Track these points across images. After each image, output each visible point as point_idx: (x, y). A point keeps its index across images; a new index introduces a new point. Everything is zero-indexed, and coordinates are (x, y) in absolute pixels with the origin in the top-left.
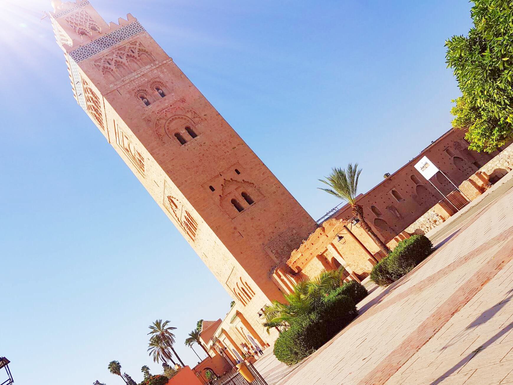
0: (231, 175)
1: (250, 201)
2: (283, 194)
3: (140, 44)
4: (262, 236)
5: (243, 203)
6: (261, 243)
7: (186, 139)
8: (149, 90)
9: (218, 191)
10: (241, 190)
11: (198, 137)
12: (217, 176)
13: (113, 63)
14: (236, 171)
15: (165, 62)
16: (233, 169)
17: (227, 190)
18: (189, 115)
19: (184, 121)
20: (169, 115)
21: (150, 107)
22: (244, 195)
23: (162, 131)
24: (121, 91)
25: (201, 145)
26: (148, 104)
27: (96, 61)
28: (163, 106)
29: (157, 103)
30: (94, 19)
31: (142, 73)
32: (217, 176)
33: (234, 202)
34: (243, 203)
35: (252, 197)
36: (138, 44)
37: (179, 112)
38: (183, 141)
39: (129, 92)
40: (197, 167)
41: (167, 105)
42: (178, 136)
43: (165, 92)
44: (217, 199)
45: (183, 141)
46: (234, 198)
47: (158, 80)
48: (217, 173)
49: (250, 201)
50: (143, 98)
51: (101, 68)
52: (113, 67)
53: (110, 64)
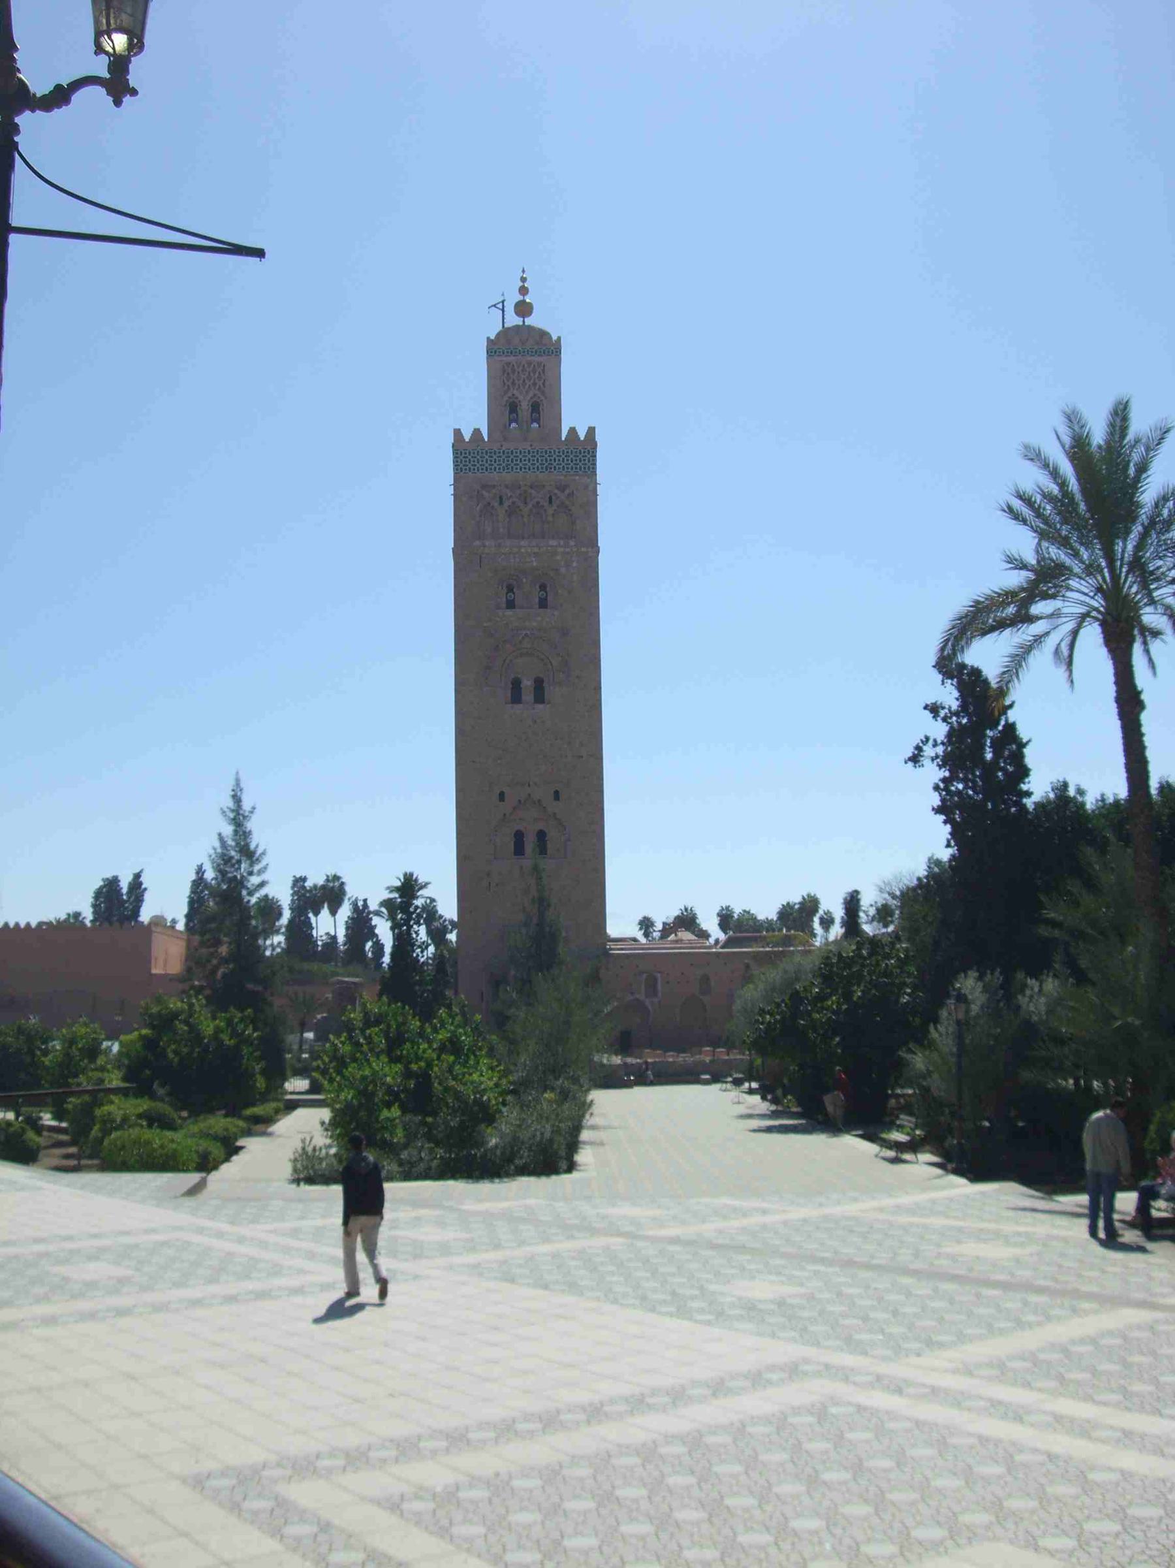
3: (571, 494)
7: (524, 698)
10: (540, 826)
11: (541, 706)
13: (506, 504)
14: (557, 793)
15: (583, 549)
21: (509, 613)
22: (541, 835)
25: (535, 722)
26: (511, 605)
27: (484, 487)
31: (536, 550)
35: (549, 845)
36: (567, 492)
38: (516, 698)
41: (535, 624)
42: (516, 685)
45: (516, 698)
46: (522, 829)
50: (510, 589)
52: (501, 513)
53: (501, 503)
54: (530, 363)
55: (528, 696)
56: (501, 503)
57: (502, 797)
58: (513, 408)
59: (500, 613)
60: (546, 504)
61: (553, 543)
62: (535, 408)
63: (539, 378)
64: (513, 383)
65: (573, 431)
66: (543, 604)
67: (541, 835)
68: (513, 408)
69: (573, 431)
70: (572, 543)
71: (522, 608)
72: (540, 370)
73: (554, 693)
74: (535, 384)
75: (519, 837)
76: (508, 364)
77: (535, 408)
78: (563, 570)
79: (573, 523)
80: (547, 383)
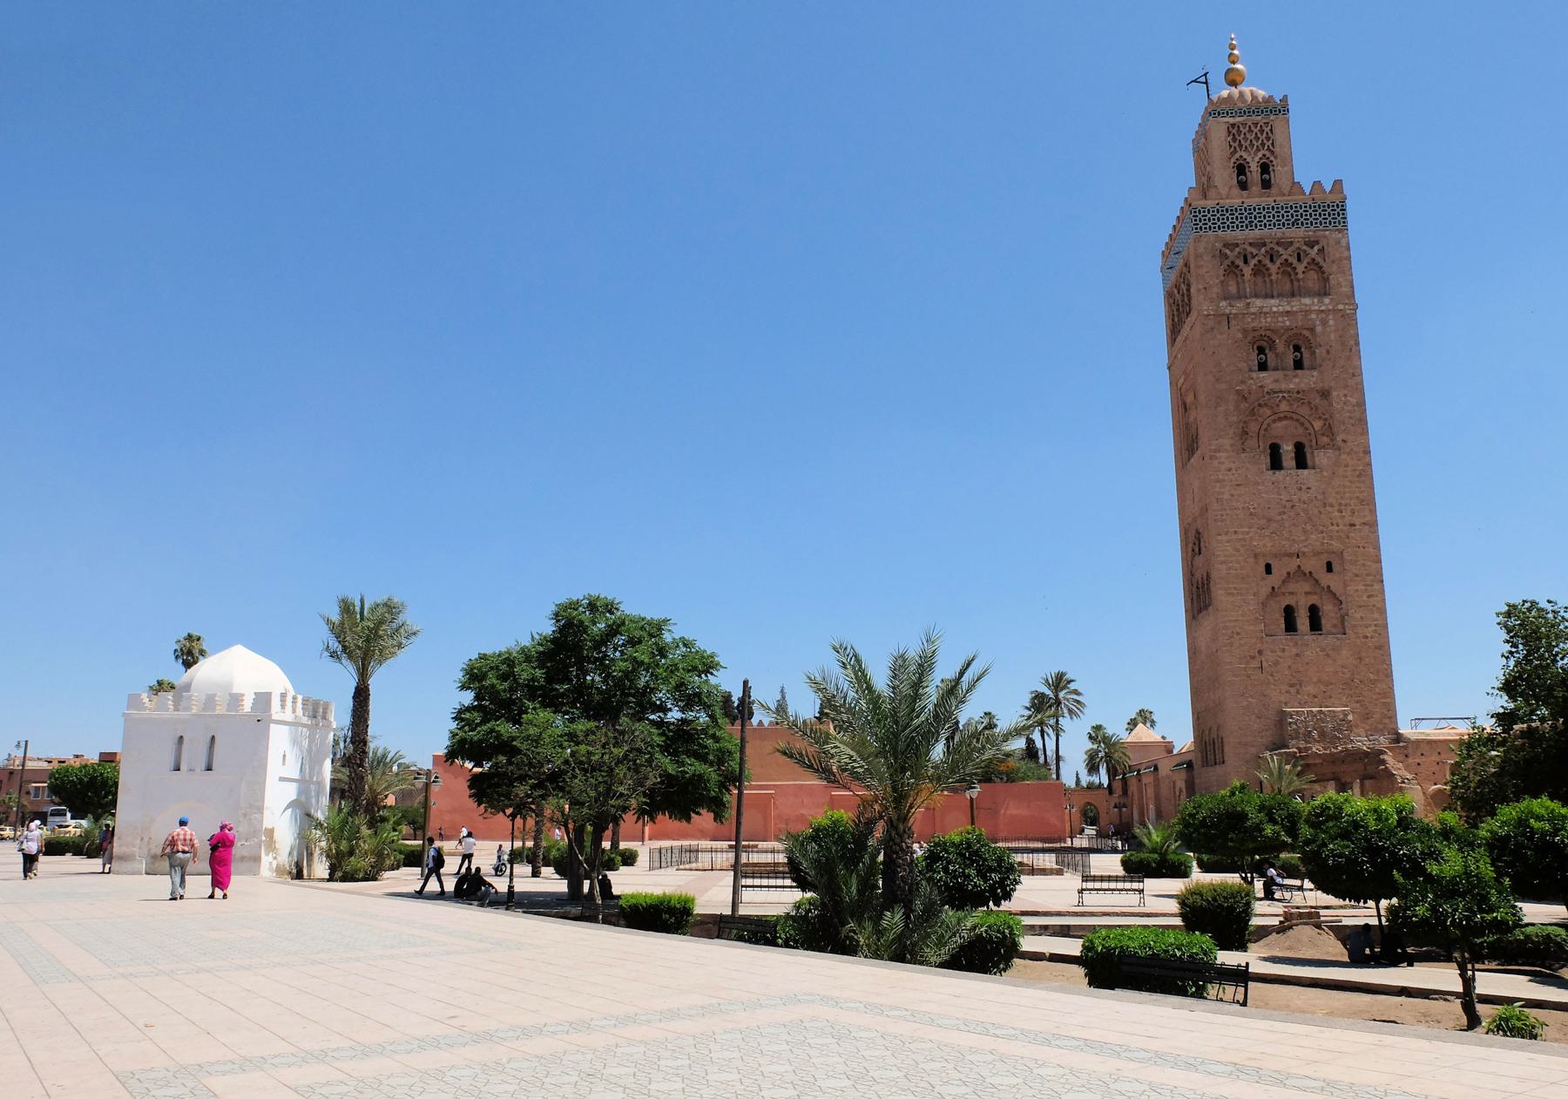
0: (1314, 565)
1: (1315, 625)
2: (1379, 648)
3: (1322, 250)
4: (1293, 690)
5: (1303, 622)
6: (1283, 699)
8: (1280, 345)
9: (1275, 579)
11: (1306, 472)
12: (1290, 555)
13: (1253, 262)
16: (1325, 558)
17: (1292, 587)
18: (1318, 425)
19: (1301, 430)
20: (1284, 407)
21: (1263, 374)
22: (1314, 613)
23: (1253, 427)
24: (1233, 322)
26: (1263, 367)
28: (1283, 387)
29: (1279, 374)
30: (1277, 150)
31: (1288, 308)
32: (1290, 555)
33: (1289, 613)
34: (1303, 622)
35: (1323, 621)
37: (1304, 411)
38: (1276, 464)
39: (1245, 332)
40: (1269, 520)
43: (1306, 362)
44: (1265, 591)
45: (1276, 464)
46: (1293, 604)
47: (1307, 333)
48: (1295, 549)
49: (1315, 625)
50: (1261, 350)
51: (1227, 262)
52: (1247, 271)
53: (1246, 262)
54: (1256, 124)
55: (1288, 459)
56: (1246, 262)
57: (1268, 569)
58: (1241, 169)
59: (1254, 375)
60: (1295, 262)
61: (1307, 301)
62: (1265, 168)
63: (1268, 138)
64: (1240, 145)
65: (1317, 184)
66: (1298, 365)
67: (1314, 613)
68: (1241, 169)
69: (1317, 184)
70: (1327, 301)
71: (1276, 369)
72: (1267, 129)
73: (1321, 458)
74: (1263, 144)
75: (1289, 613)
76: (1233, 125)
77: (1265, 168)
78: (1319, 329)
79: (1326, 280)
80: (1277, 144)
